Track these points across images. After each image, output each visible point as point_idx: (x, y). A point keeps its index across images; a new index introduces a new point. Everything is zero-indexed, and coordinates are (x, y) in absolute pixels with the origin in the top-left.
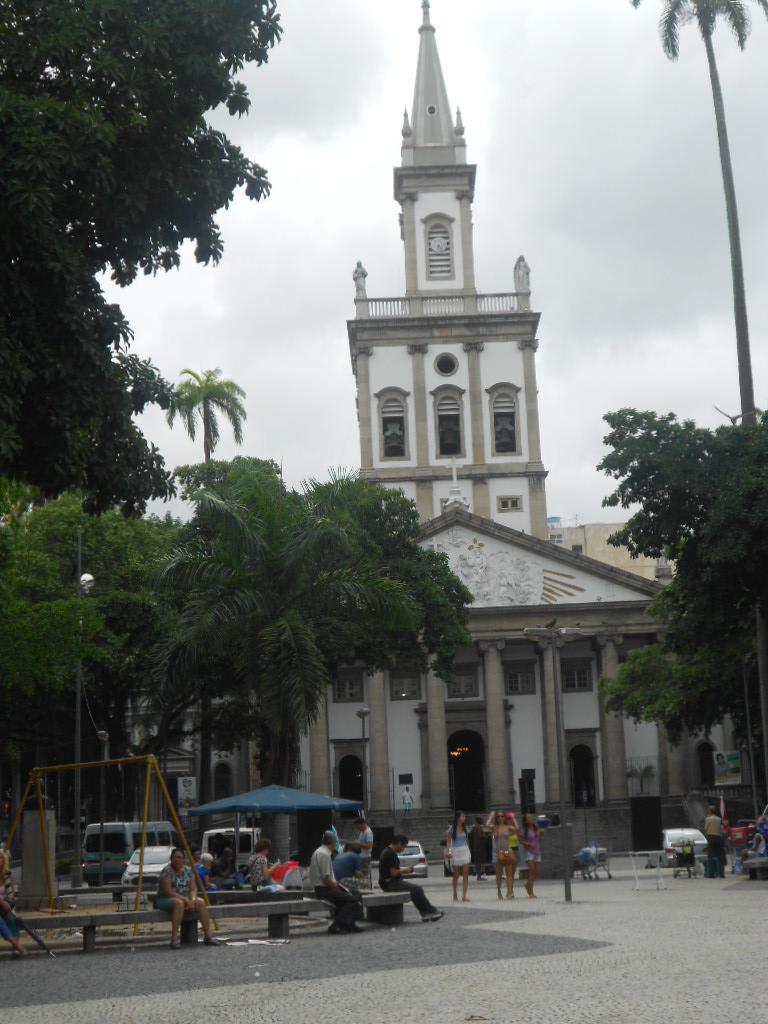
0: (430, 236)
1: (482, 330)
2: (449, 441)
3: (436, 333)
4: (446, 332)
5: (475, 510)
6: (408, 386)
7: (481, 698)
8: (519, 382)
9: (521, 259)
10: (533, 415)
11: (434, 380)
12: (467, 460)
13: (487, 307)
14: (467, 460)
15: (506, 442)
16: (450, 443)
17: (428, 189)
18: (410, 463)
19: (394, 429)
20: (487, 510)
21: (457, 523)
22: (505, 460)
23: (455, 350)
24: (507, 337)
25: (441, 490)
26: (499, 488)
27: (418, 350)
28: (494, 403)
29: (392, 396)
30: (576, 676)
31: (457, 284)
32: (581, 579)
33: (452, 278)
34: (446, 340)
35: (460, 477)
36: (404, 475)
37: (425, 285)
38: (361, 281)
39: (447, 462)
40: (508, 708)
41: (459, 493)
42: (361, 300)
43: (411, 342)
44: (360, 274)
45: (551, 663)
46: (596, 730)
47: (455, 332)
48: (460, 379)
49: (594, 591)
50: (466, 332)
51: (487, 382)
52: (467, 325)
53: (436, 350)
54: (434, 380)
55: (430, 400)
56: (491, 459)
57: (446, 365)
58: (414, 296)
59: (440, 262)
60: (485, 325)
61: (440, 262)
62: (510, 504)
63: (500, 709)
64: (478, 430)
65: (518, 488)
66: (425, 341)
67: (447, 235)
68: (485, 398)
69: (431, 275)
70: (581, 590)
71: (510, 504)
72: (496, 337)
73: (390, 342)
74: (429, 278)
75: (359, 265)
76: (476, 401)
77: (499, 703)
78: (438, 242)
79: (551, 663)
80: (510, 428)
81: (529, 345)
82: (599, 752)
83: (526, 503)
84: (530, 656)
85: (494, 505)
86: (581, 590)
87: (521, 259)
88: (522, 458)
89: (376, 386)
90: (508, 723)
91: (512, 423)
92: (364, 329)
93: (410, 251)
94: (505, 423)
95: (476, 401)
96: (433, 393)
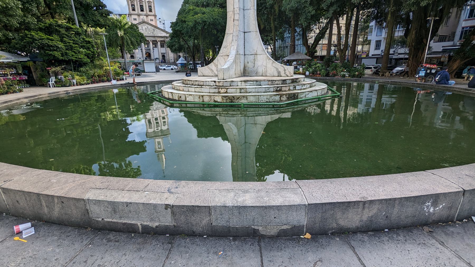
2: (142, 9)
10: (154, 6)
12: (145, 13)
14: (145, 13)
15: (151, 11)
16: (142, 10)
19: (133, 6)
20: (148, 21)
22: (150, 13)
25: (141, 17)
26: (150, 18)
30: (162, 46)
32: (162, 32)
41: (143, 18)
49: (164, 34)
62: (152, 20)
64: (146, 8)
65: (153, 18)
68: (147, 3)
71: (152, 20)
76: (145, 3)
83: (154, 20)
85: (149, 20)
88: (153, 13)
94: (150, 7)
95: (145, 3)
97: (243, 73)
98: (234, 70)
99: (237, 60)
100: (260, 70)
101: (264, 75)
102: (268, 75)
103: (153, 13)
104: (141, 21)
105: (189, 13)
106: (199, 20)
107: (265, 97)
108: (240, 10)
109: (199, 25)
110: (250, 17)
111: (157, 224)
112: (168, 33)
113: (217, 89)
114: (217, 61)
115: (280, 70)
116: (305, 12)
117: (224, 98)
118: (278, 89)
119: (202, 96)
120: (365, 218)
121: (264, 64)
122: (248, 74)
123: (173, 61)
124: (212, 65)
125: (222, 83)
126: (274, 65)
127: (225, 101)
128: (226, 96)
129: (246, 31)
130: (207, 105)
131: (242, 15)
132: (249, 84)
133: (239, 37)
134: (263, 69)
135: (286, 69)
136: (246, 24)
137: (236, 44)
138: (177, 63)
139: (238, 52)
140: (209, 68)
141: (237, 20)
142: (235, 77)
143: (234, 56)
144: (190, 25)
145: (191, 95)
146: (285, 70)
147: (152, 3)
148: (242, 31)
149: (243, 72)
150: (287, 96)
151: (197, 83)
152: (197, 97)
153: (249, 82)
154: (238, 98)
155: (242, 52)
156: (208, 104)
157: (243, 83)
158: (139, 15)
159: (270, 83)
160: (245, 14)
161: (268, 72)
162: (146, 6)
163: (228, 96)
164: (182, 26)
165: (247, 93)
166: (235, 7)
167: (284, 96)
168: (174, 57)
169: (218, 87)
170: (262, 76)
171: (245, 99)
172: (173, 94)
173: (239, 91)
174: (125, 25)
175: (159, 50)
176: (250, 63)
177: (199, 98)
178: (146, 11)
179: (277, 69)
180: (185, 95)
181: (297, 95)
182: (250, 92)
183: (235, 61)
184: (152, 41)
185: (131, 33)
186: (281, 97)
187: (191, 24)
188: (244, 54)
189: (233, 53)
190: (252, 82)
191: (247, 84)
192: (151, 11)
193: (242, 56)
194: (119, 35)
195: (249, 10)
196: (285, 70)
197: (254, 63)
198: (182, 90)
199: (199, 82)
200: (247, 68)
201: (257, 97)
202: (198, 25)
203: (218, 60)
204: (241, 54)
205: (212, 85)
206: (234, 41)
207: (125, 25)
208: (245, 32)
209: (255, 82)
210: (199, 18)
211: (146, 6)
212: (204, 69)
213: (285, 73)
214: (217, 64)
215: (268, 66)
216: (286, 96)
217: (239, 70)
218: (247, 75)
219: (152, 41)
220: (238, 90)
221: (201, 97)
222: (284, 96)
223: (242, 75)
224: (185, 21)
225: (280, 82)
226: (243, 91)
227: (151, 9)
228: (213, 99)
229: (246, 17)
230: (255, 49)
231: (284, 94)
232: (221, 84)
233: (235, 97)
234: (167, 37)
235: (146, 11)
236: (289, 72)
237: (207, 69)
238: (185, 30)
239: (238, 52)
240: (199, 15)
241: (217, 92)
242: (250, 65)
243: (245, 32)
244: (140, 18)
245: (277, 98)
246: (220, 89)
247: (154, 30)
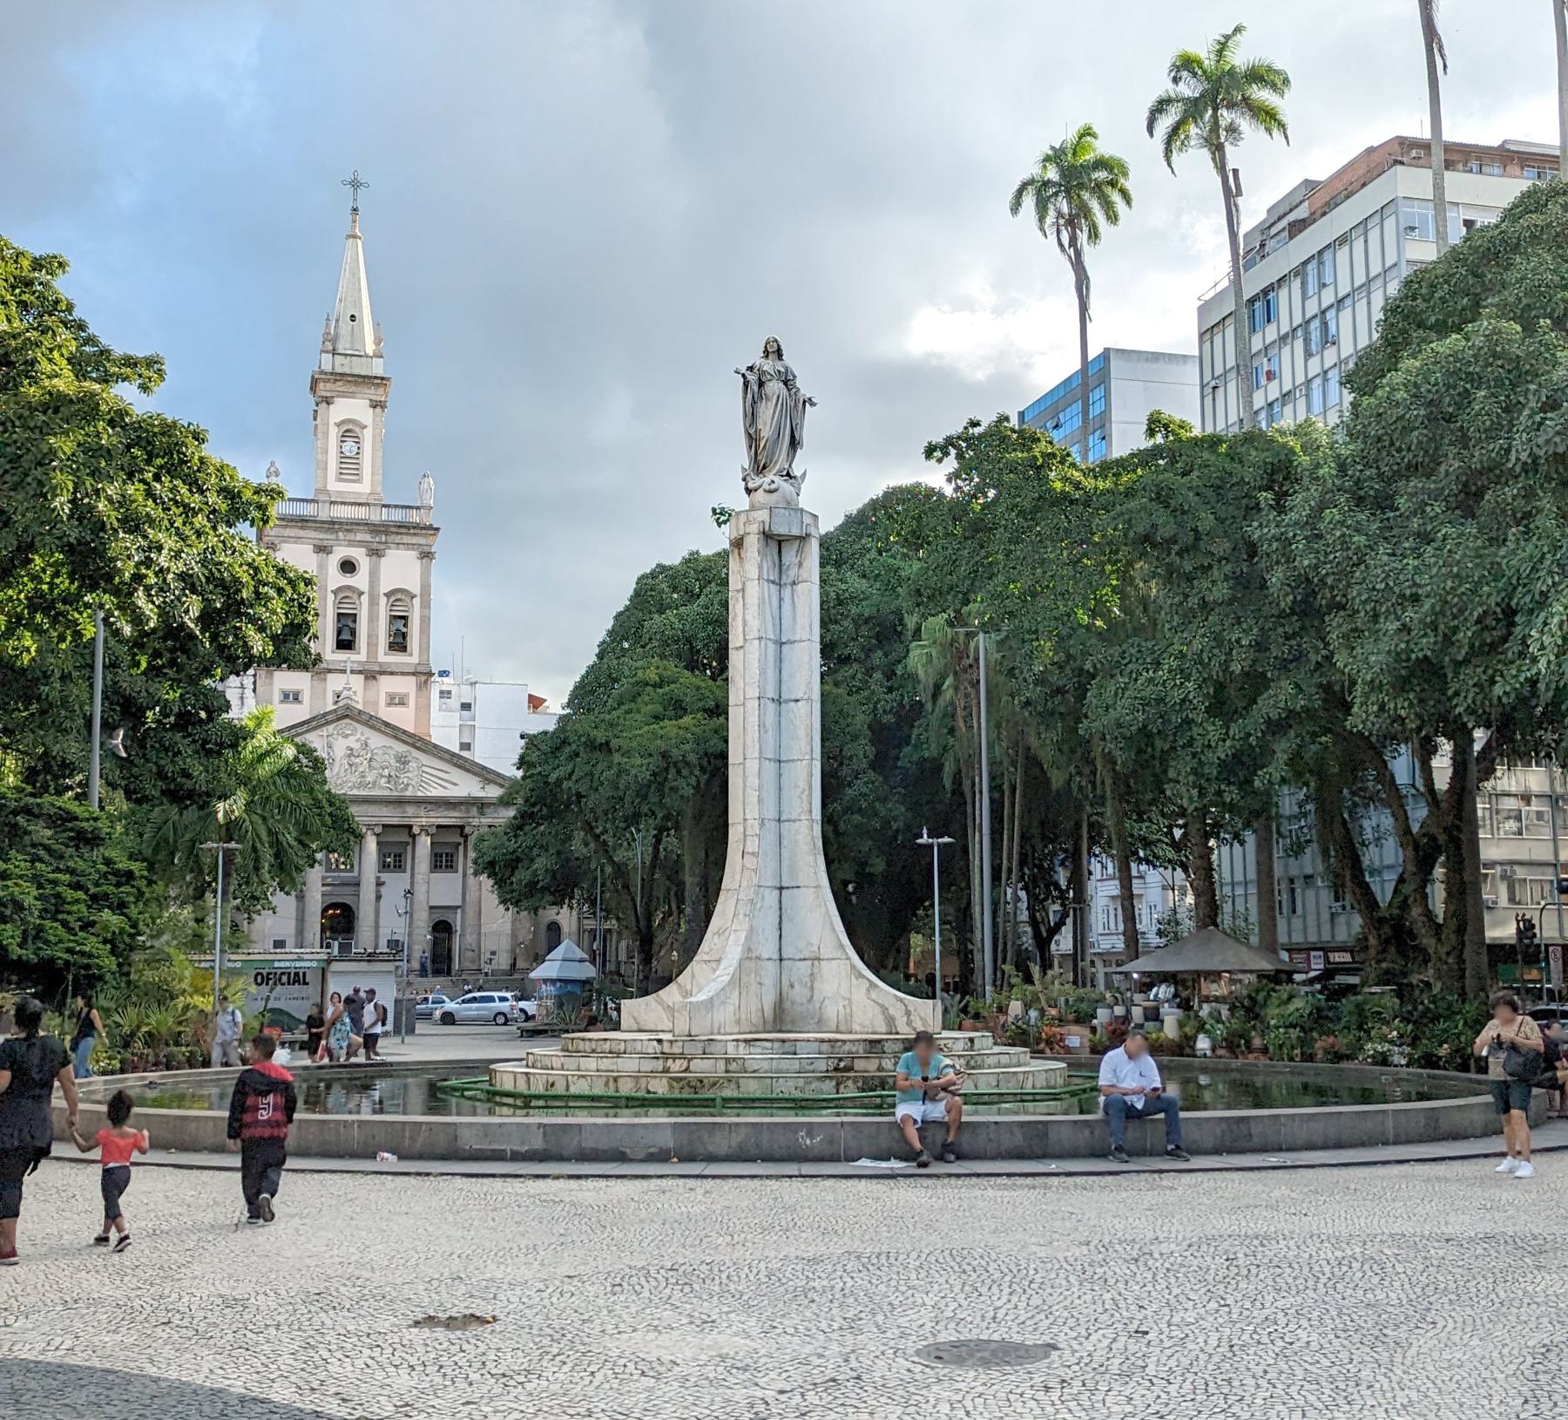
2: (346, 636)
4: (351, 536)
5: (365, 703)
7: (355, 874)
8: (416, 590)
10: (425, 621)
15: (399, 643)
17: (344, 395)
20: (377, 703)
22: (397, 659)
23: (358, 555)
24: (409, 546)
25: (335, 682)
26: (387, 684)
30: (443, 861)
32: (456, 775)
34: (351, 543)
35: (352, 672)
39: (343, 656)
40: (379, 884)
43: (316, 542)
46: (458, 907)
47: (360, 537)
48: (360, 580)
49: (467, 787)
51: (385, 587)
53: (341, 552)
56: (385, 657)
57: (348, 567)
62: (397, 700)
63: (373, 888)
64: (373, 629)
65: (407, 685)
66: (331, 543)
68: (383, 600)
69: (340, 476)
70: (455, 784)
71: (397, 700)
76: (373, 602)
77: (373, 881)
78: (350, 446)
80: (404, 630)
82: (458, 928)
83: (412, 701)
84: (405, 838)
85: (383, 700)
86: (455, 784)
90: (379, 897)
91: (405, 625)
94: (400, 624)
95: (373, 602)
97: (775, 1022)
98: (730, 1009)
99: (744, 978)
100: (832, 1011)
101: (842, 1028)
102: (856, 1027)
104: (331, 707)
105: (633, 700)
106: (687, 747)
107: (791, 1083)
108: (762, 824)
109: (685, 772)
110: (796, 841)
111: (526, 1148)
112: (490, 781)
113: (661, 1062)
114: (689, 979)
115: (892, 1011)
116: (1190, 743)
117: (675, 1084)
118: (842, 1065)
119: (616, 1079)
120: (734, 1144)
121: (844, 991)
122: (793, 1022)
123: (503, 962)
124: (670, 994)
125: (680, 1044)
126: (874, 996)
127: (677, 1091)
128: (681, 1079)
129: (784, 885)
130: (623, 1101)
131: (771, 838)
132: (759, 1050)
133: (758, 906)
134: (841, 1009)
135: (911, 1008)
136: (785, 863)
137: (746, 926)
138: (533, 975)
139: (749, 950)
140: (661, 1002)
141: (753, 854)
142: (736, 1030)
143: (735, 963)
144: (633, 772)
145: (583, 1076)
146: (908, 1013)
147: (417, 601)
148: (770, 884)
149: (775, 1018)
150: (860, 1084)
151: (607, 1046)
152: (601, 1082)
153: (759, 1043)
154: (715, 1084)
155: (768, 949)
156: (627, 1098)
157: (742, 1045)
159: (825, 1047)
160: (784, 833)
161: (855, 1019)
162: (373, 618)
163: (685, 1078)
164: (588, 768)
165: (746, 1072)
166: (747, 817)
167: (850, 1083)
168: (514, 935)
169: (666, 1056)
170: (837, 1032)
171: (733, 1086)
172: (532, 1077)
173: (723, 1068)
174: (261, 758)
175: (420, 889)
176: (797, 986)
177: (607, 1084)
178: (372, 645)
179: (884, 1010)
180: (567, 1076)
181: (891, 1081)
182: (754, 1072)
183: (737, 981)
184: (378, 830)
185: (289, 801)
186: (838, 1084)
187: (639, 768)
188: (776, 956)
189: (733, 954)
190: (768, 1045)
191: (752, 1050)
192: (399, 643)
193: (769, 963)
194: (220, 815)
195: (794, 821)
196: (908, 1013)
197: (812, 989)
198: (559, 1066)
199: (613, 1043)
200: (787, 1005)
201: (769, 1081)
202: (679, 772)
203: (693, 976)
204: (766, 956)
205: (650, 1051)
206: (741, 916)
207: (261, 758)
208: (781, 888)
209: (776, 1045)
210: (684, 741)
211: (373, 618)
212: (643, 1006)
213: (909, 1023)
214: (689, 988)
215: (855, 998)
216: (855, 1082)
217: (754, 1006)
218: (789, 1028)
219: (378, 830)
220: (721, 1065)
221: (611, 1083)
222: (850, 1083)
223: (769, 1027)
224: (606, 747)
225: (860, 1048)
226: (733, 1066)
227: (404, 635)
228: (644, 1086)
229: (785, 843)
230: (815, 941)
231: (849, 1078)
232: (677, 1049)
233: (705, 1081)
234: (481, 805)
235: (372, 645)
236: (921, 1019)
237: (654, 1004)
238: (606, 792)
239: (749, 950)
240: (687, 720)
241: (661, 1069)
242: (798, 994)
243: (781, 888)
244: (325, 691)
245: (829, 1086)
246: (670, 1061)
247: (403, 761)
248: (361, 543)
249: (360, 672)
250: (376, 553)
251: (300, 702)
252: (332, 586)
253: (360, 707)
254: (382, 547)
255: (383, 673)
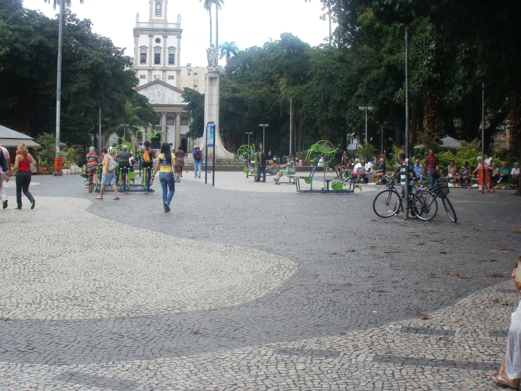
0: (157, 5)
1: (168, 32)
2: (157, 60)
3: (156, 32)
4: (158, 32)
6: (148, 46)
7: (160, 125)
8: (176, 47)
9: (179, 14)
10: (179, 55)
11: (155, 44)
12: (162, 66)
13: (170, 27)
14: (162, 66)
15: (171, 62)
16: (157, 61)
18: (147, 65)
20: (165, 79)
21: (158, 83)
22: (171, 66)
23: (161, 37)
24: (174, 35)
25: (154, 73)
27: (151, 36)
28: (169, 51)
29: (143, 47)
31: (162, 18)
33: (161, 16)
34: (158, 34)
35: (159, 70)
36: (145, 68)
37: (154, 18)
38: (138, 17)
40: (167, 128)
41: (158, 74)
42: (138, 23)
43: (149, 34)
44: (138, 15)
45: (178, 118)
47: (161, 32)
48: (161, 44)
50: (163, 32)
51: (168, 46)
52: (164, 31)
53: (156, 37)
54: (155, 44)
55: (153, 49)
56: (168, 66)
57: (158, 41)
58: (152, 21)
59: (158, 12)
60: (169, 31)
61: (158, 12)
62: (171, 77)
64: (164, 58)
65: (174, 73)
67: (161, 5)
71: (171, 77)
72: (171, 34)
73: (144, 34)
74: (155, 16)
75: (138, 13)
76: (165, 50)
79: (178, 118)
81: (179, 37)
83: (175, 78)
84: (174, 116)
87: (179, 14)
88: (175, 66)
89: (140, 45)
91: (174, 57)
92: (137, 30)
93: (151, 8)
95: (165, 50)
96: (154, 48)
103: (175, 66)
104: (153, 80)
147: (176, 50)
158: (150, 70)
162: (165, 55)
178: (164, 62)
184: (166, 113)
192: (171, 62)
211: (165, 55)
219: (166, 113)
235: (164, 62)
244: (152, 76)
248: (161, 34)
249: (161, 70)
250: (165, 37)
251: (145, 78)
252: (154, 46)
253: (161, 80)
254: (167, 35)
255: (167, 70)
